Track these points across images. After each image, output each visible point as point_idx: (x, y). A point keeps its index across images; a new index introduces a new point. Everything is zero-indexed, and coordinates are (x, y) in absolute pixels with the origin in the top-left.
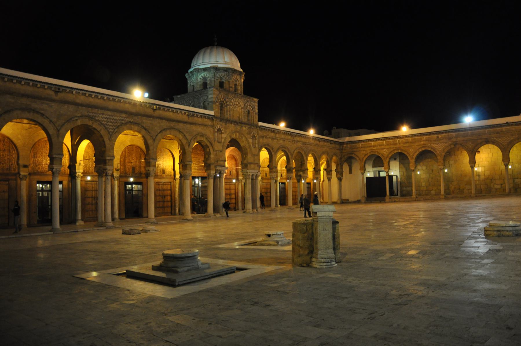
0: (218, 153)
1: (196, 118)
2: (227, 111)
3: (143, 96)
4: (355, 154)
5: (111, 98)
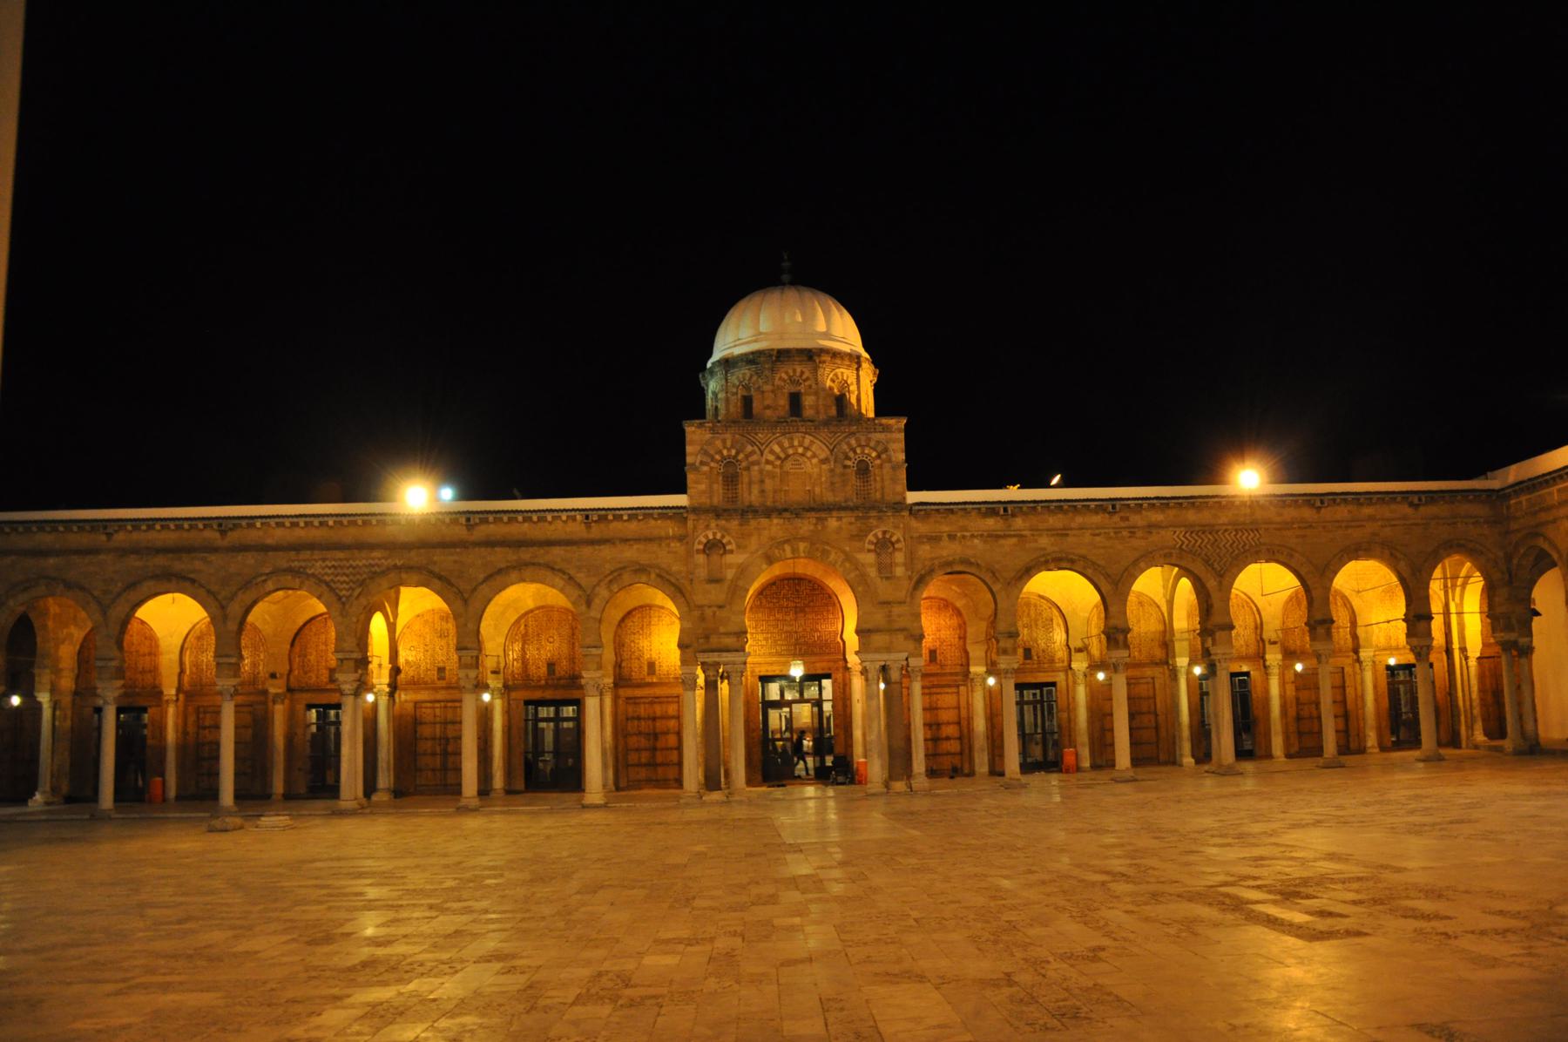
0: (709, 612)
1: (617, 525)
2: (750, 483)
3: (437, 499)
4: (1546, 538)
5: (345, 521)
